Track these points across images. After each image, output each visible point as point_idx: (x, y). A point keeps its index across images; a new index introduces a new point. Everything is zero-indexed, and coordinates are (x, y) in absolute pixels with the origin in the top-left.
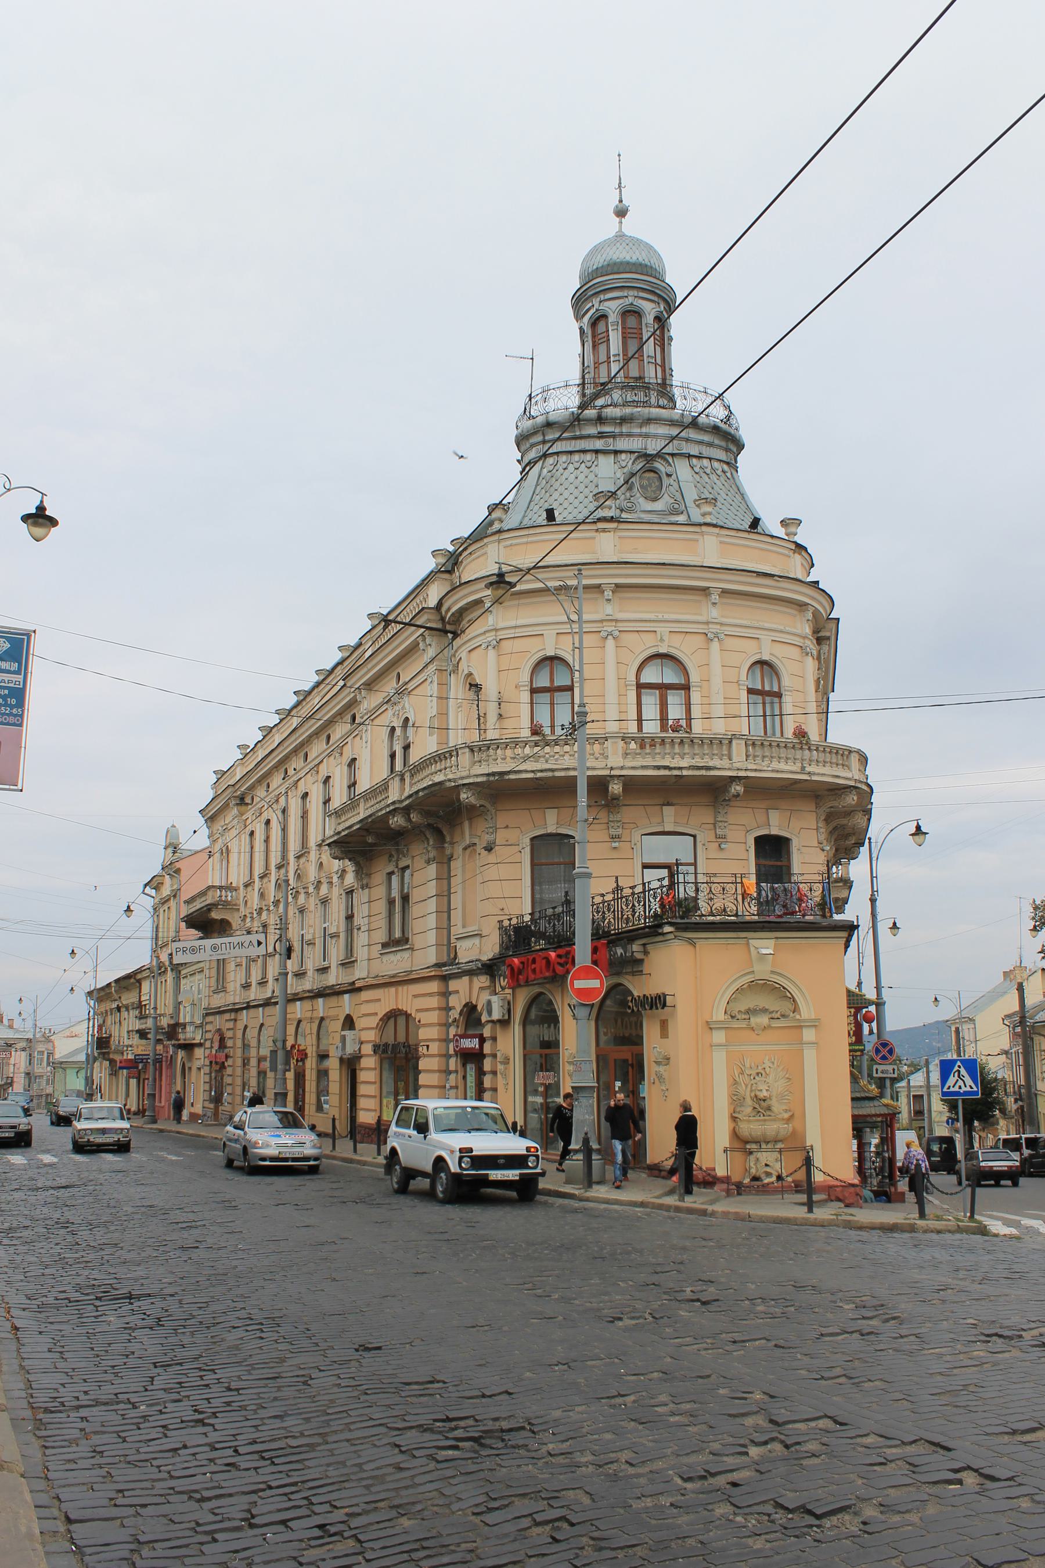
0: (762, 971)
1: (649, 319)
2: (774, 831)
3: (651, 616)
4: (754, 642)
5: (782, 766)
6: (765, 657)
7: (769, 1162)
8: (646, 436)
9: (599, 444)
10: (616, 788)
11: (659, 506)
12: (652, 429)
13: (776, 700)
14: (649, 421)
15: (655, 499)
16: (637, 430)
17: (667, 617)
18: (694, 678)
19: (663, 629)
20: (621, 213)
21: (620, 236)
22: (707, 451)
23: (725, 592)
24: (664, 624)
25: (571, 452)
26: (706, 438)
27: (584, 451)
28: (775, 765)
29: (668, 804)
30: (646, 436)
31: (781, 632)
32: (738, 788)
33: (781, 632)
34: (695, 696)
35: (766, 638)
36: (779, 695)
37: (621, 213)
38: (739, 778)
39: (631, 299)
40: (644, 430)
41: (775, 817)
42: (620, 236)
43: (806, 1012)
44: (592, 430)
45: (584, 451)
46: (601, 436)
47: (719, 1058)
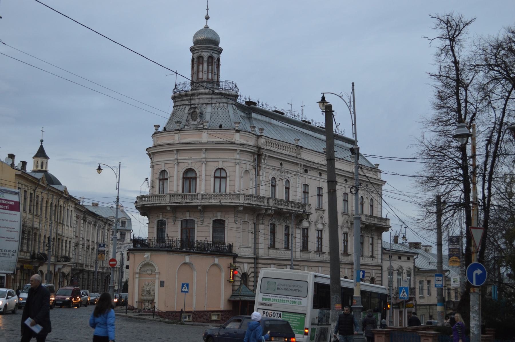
0: (148, 261)
1: (206, 59)
2: (219, 218)
3: (187, 158)
4: (217, 163)
5: (213, 201)
6: (220, 167)
7: (148, 305)
8: (199, 99)
9: (187, 102)
10: (168, 208)
11: (196, 123)
12: (201, 96)
13: (225, 179)
14: (199, 94)
15: (195, 121)
16: (197, 97)
17: (193, 157)
18: (198, 175)
19: (190, 161)
20: (207, 18)
21: (207, 27)
22: (218, 100)
23: (206, 150)
24: (188, 160)
25: (180, 105)
26: (218, 97)
27: (183, 105)
28: (210, 201)
29: (188, 211)
30: (199, 99)
31: (226, 159)
32: (199, 208)
33: (226, 159)
34: (198, 180)
35: (220, 161)
36: (225, 178)
37: (207, 18)
38: (200, 205)
39: (200, 53)
40: (199, 97)
41: (219, 214)
42: (207, 27)
43: (157, 271)
44: (185, 98)
45: (183, 105)
46: (187, 100)
47: (137, 281)
